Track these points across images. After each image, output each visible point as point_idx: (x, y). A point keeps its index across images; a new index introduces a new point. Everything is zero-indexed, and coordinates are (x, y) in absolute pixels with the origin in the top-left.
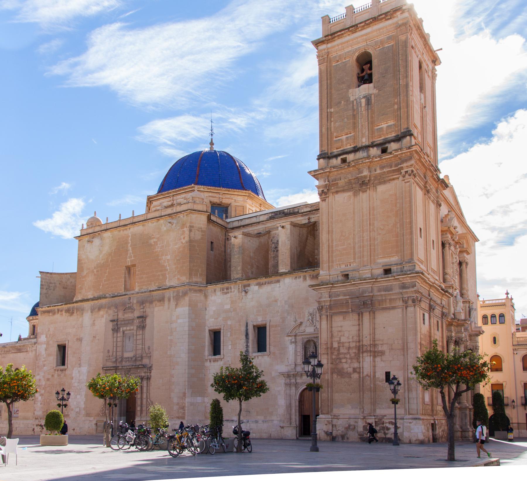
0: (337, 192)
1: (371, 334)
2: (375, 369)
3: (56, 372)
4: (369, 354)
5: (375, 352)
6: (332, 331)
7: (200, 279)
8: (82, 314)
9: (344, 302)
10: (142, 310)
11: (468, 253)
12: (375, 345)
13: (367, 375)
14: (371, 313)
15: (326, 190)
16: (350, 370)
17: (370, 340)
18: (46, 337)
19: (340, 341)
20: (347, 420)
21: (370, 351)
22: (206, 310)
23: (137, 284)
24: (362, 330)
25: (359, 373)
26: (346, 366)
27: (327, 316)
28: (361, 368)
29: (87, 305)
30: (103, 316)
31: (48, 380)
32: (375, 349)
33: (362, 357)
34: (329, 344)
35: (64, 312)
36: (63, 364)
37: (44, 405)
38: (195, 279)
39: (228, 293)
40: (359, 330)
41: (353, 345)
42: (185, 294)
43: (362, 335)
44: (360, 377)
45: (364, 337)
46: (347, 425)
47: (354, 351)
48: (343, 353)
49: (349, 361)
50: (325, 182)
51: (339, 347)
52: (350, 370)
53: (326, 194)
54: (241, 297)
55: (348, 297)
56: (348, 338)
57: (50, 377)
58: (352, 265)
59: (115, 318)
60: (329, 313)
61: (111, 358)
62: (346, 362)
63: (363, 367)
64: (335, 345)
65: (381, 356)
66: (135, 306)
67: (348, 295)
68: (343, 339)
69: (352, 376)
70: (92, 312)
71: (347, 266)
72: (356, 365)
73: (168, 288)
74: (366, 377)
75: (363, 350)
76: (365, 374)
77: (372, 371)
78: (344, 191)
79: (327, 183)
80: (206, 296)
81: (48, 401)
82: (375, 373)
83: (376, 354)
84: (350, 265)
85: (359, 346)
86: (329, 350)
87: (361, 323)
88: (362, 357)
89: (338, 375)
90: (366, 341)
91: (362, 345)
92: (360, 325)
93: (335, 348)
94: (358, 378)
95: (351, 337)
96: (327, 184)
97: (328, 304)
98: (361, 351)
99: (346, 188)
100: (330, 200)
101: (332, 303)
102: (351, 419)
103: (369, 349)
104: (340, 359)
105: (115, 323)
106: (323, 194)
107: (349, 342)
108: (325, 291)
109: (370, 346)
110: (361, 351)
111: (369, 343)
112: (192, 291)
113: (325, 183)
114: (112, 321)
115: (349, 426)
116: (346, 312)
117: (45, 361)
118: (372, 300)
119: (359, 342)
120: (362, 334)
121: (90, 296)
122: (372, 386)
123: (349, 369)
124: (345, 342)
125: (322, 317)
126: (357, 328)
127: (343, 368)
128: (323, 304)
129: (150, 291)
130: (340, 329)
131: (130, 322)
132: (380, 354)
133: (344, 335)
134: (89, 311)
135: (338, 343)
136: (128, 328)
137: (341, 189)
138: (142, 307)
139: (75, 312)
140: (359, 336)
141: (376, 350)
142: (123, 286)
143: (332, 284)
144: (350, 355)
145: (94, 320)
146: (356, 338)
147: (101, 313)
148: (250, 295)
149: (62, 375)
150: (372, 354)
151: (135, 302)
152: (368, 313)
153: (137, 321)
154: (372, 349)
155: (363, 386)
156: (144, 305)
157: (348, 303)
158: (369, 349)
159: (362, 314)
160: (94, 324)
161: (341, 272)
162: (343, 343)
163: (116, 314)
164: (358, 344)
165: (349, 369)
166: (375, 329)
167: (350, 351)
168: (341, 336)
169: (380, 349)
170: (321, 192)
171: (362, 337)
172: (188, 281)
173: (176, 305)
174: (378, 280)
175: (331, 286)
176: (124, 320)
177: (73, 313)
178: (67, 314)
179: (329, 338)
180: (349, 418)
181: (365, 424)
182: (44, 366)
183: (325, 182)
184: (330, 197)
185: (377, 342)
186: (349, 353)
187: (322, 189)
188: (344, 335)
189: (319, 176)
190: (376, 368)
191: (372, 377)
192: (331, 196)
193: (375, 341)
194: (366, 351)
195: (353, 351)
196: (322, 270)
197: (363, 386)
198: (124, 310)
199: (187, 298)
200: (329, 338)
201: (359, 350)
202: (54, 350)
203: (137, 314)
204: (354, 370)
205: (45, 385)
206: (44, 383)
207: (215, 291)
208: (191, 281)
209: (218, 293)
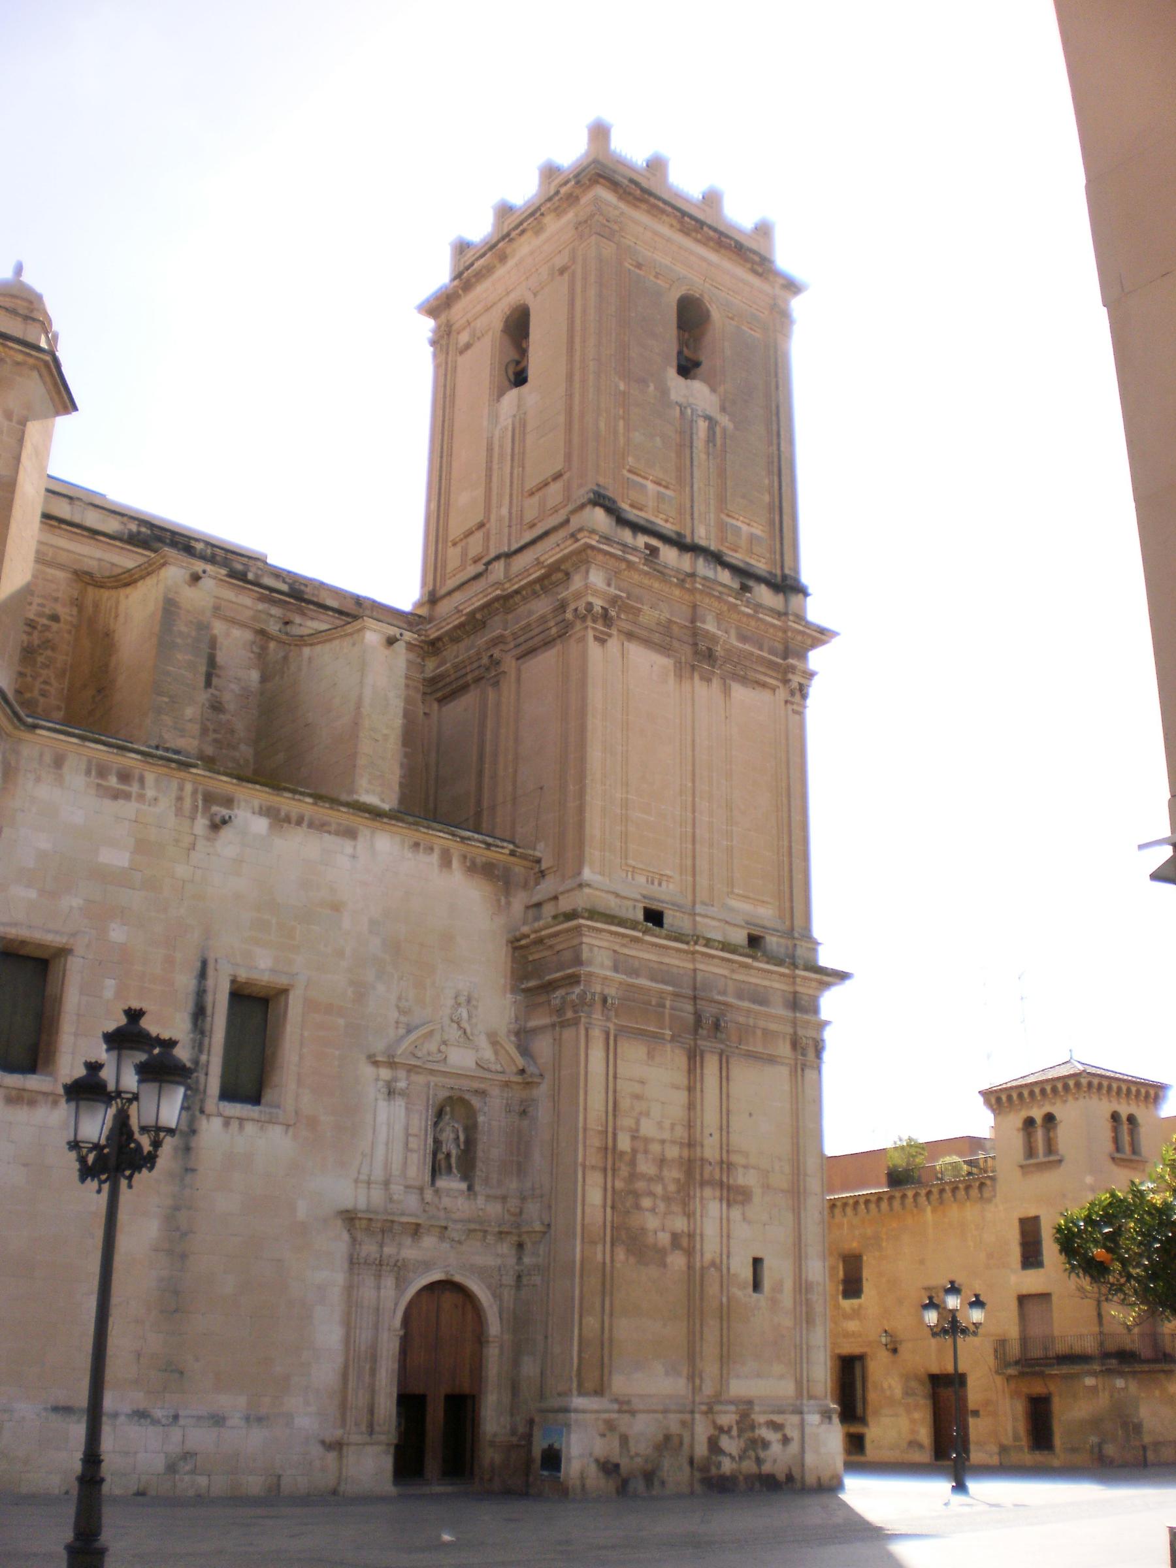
0: (630, 636)
4: (718, 1194)
13: (713, 1264)
16: (664, 1238)
19: (637, 1130)
20: (660, 1416)
21: (721, 1184)
26: (652, 1223)
27: (607, 1034)
33: (702, 1198)
39: (127, 796)
40: (691, 1106)
41: (673, 1152)
45: (707, 1132)
46: (660, 1437)
48: (643, 1176)
49: (661, 1206)
51: (634, 1151)
52: (664, 1238)
54: (187, 840)
55: (671, 989)
56: (660, 1125)
58: (664, 884)
60: (612, 1026)
62: (653, 1210)
63: (702, 1235)
64: (624, 1143)
65: (743, 1203)
68: (648, 1128)
69: (669, 1259)
71: (653, 883)
72: (679, 1224)
75: (702, 1174)
76: (708, 1256)
78: (647, 642)
83: (734, 1195)
84: (660, 884)
85: (690, 1161)
88: (702, 1198)
89: (629, 1251)
90: (710, 1150)
91: (702, 1159)
92: (692, 1088)
93: (622, 1153)
94: (684, 1268)
95: (667, 1124)
102: (672, 1416)
104: (636, 1195)
107: (663, 1142)
108: (605, 944)
115: (667, 1438)
116: (655, 1036)
119: (691, 1145)
120: (702, 1123)
122: (724, 1300)
123: (661, 1235)
124: (653, 1140)
125: (590, 1032)
126: (682, 1097)
127: (643, 1230)
130: (637, 1089)
132: (740, 1198)
133: (647, 1114)
135: (634, 1138)
137: (644, 633)
140: (690, 1126)
144: (665, 1188)
146: (681, 1133)
148: (228, 843)
155: (702, 1299)
157: (664, 1006)
158: (717, 1177)
161: (644, 897)
162: (647, 1141)
164: (685, 1153)
165: (661, 1235)
168: (641, 1113)
169: (742, 1178)
171: (702, 1132)
180: (665, 1411)
181: (712, 1431)
185: (735, 1158)
186: (660, 1178)
188: (648, 1114)
189: (600, 557)
195: (673, 1174)
201: (689, 1173)
207: (59, 762)
209: (76, 779)
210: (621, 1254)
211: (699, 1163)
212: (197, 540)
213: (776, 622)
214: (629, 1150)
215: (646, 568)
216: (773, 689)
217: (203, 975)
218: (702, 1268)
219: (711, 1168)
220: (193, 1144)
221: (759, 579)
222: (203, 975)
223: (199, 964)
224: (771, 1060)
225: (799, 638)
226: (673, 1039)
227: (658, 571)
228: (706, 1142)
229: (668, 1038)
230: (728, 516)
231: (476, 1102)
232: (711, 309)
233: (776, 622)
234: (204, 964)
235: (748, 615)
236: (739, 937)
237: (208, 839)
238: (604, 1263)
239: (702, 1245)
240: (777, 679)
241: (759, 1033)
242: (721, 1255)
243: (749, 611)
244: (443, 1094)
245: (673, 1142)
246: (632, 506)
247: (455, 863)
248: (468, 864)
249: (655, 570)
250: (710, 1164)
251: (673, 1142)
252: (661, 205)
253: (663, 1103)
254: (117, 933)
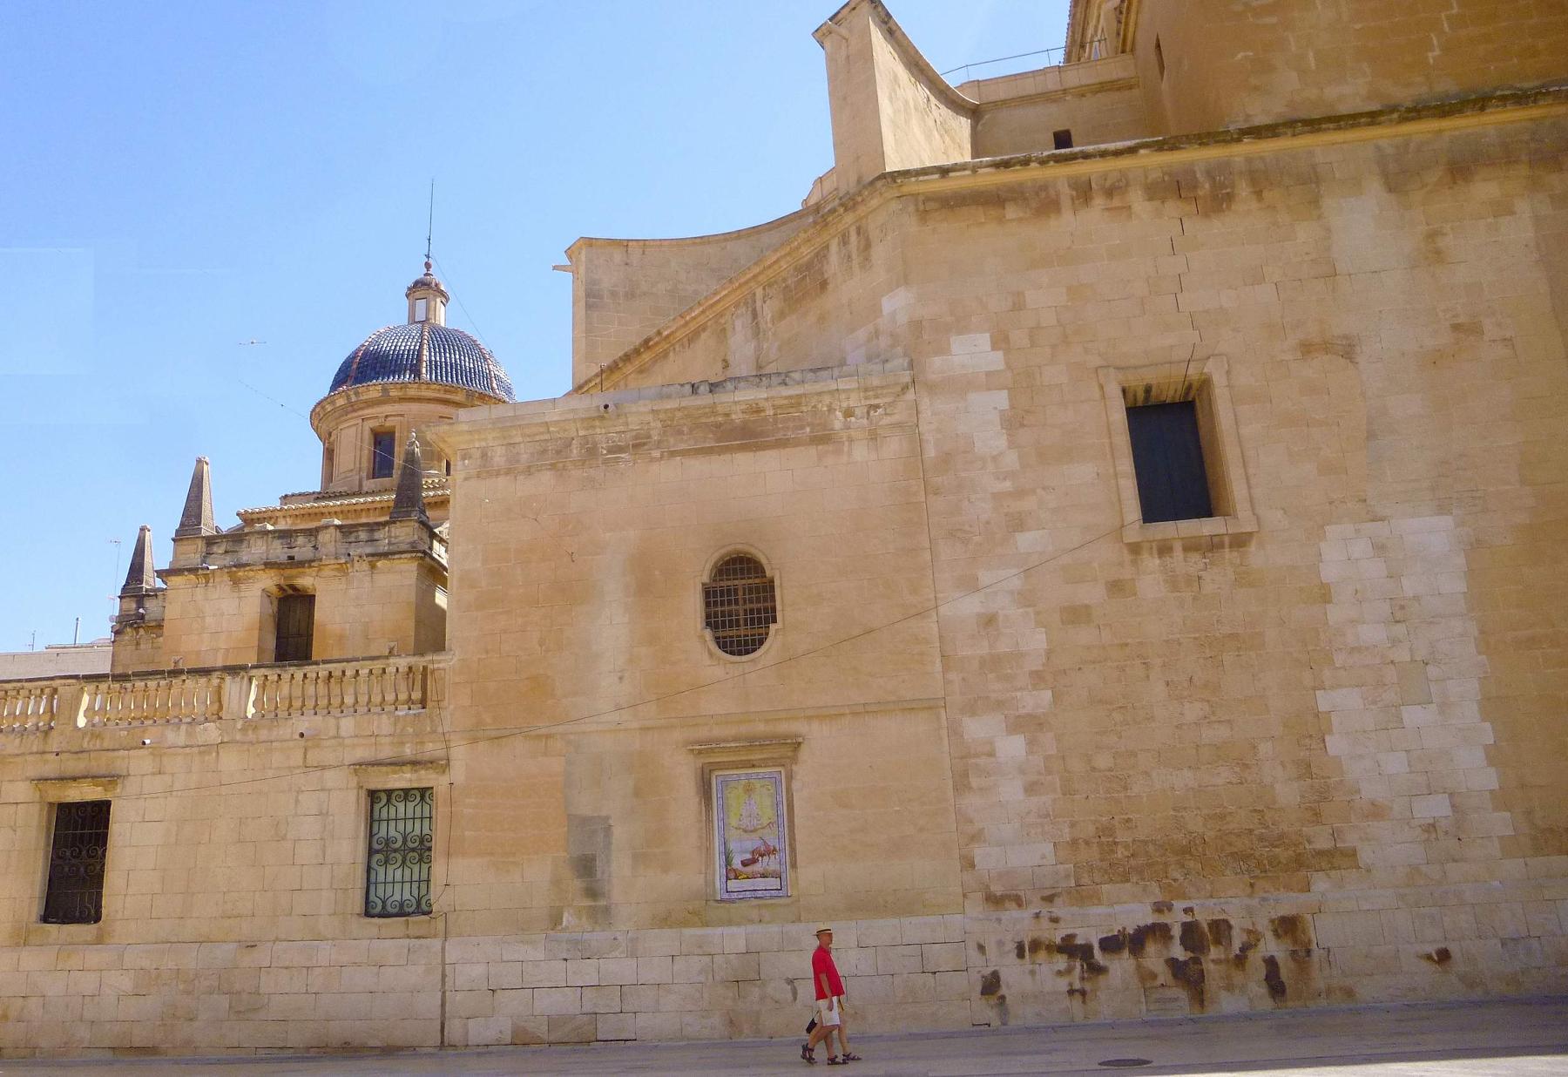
3: (1152, 562)
8: (1315, 202)
30: (1503, 209)
31: (1076, 615)
35: (1136, 198)
37: (1068, 791)
57: (1091, 594)
81: (1103, 761)
117: (1020, 493)
134: (1375, 186)
139: (1243, 190)
145: (1432, 236)
147: (1485, 189)
149: (1218, 576)
160: (1438, 252)
178: (1173, 208)
182: (1018, 523)
205: (1049, 653)
206: (1036, 642)
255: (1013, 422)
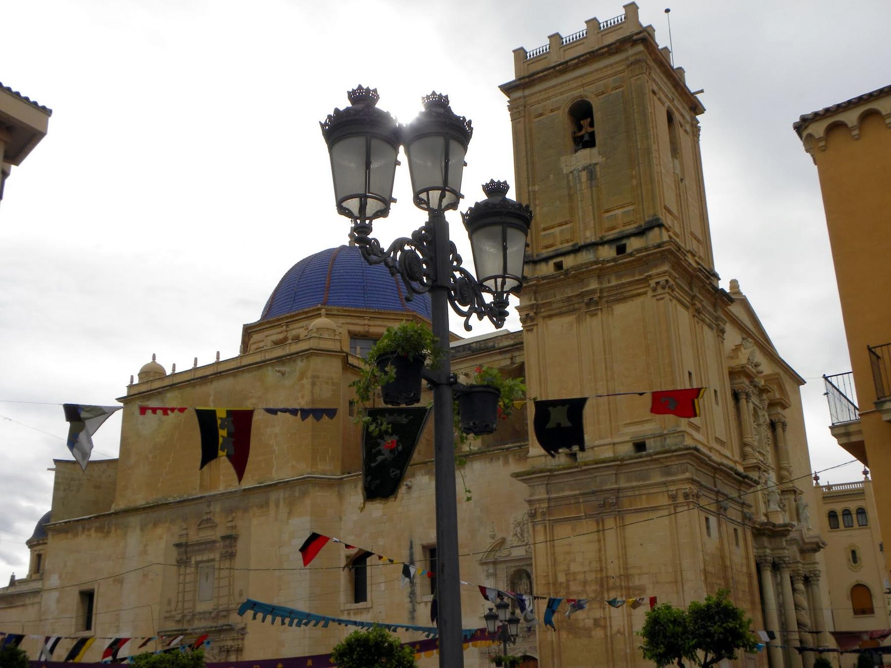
0: (550, 317)
1: (621, 555)
2: (631, 619)
5: (628, 588)
6: (554, 554)
7: (329, 468)
8: (125, 534)
9: (573, 501)
10: (230, 524)
11: (784, 407)
12: (628, 577)
13: (619, 632)
14: (618, 519)
15: (532, 314)
16: (589, 623)
17: (619, 568)
18: (60, 578)
19: (569, 570)
21: (621, 588)
22: (341, 520)
23: (221, 477)
24: (605, 551)
25: (605, 627)
27: (545, 527)
28: (608, 619)
29: (134, 521)
30: (161, 538)
32: (628, 582)
34: (550, 577)
36: (88, 626)
38: (320, 467)
40: (600, 550)
41: (591, 577)
42: (304, 494)
43: (606, 560)
44: (606, 636)
47: (594, 587)
50: (530, 300)
51: (568, 581)
52: (589, 623)
53: (532, 319)
59: (183, 540)
61: (173, 613)
63: (610, 617)
64: (562, 578)
66: (217, 519)
67: (578, 489)
68: (574, 568)
69: (593, 633)
70: (142, 530)
73: (275, 484)
74: (616, 634)
75: (608, 585)
76: (615, 629)
77: (626, 622)
78: (561, 314)
79: (533, 302)
80: (341, 496)
82: (632, 627)
85: (602, 579)
86: (551, 587)
87: (602, 538)
90: (613, 569)
91: (607, 577)
93: (561, 583)
96: (533, 305)
97: (545, 505)
98: (606, 586)
99: (564, 309)
100: (540, 330)
101: (552, 504)
103: (618, 584)
105: (183, 549)
106: (529, 321)
107: (585, 572)
109: (620, 579)
110: (606, 586)
111: (618, 574)
112: (317, 488)
113: (531, 303)
114: (178, 546)
118: (617, 498)
119: (601, 570)
121: (140, 502)
123: (587, 621)
124: (578, 573)
128: (537, 506)
129: (245, 490)
131: (209, 545)
132: (638, 592)
133: (574, 560)
135: (566, 574)
136: (205, 558)
137: (557, 311)
138: (230, 518)
140: (601, 561)
141: (631, 585)
142: (198, 481)
143: (550, 470)
146: (595, 565)
147: (159, 531)
150: (624, 593)
151: (218, 509)
152: (613, 519)
153: (220, 545)
154: (623, 584)
155: (612, 651)
156: (234, 515)
158: (618, 584)
159: (603, 521)
162: (574, 573)
163: (185, 532)
164: (599, 576)
165: (587, 621)
166: (625, 548)
167: (588, 588)
169: (636, 582)
170: (524, 317)
171: (606, 563)
172: (309, 470)
173: (290, 513)
174: (626, 462)
175: (548, 473)
176: (199, 544)
177: (109, 532)
178: (100, 535)
179: (550, 567)
183: (530, 300)
184: (539, 325)
185: (631, 571)
187: (525, 313)
188: (574, 560)
190: (633, 617)
191: (627, 634)
192: (540, 321)
193: (627, 568)
194: (613, 588)
196: (532, 446)
197: (612, 651)
198: (199, 525)
199: (308, 501)
200: (550, 567)
201: (602, 586)
202: (73, 600)
203: (220, 532)
204: (596, 622)
208: (314, 470)
210: (564, 635)
211: (605, 579)
212: (472, 343)
213: (631, 259)
214: (565, 581)
215: (545, 281)
216: (645, 293)
217: (411, 547)
218: (611, 635)
219: (613, 580)
220: (415, 615)
221: (628, 236)
222: (411, 547)
223: (409, 544)
224: (655, 509)
225: (651, 257)
226: (586, 517)
227: (552, 278)
228: (608, 567)
229: (584, 517)
230: (607, 212)
231: (528, 569)
232: (588, 100)
233: (631, 259)
234: (411, 543)
235: (613, 266)
236: (627, 449)
237: (407, 493)
238: (552, 642)
239: (610, 622)
240: (646, 287)
241: (644, 497)
242: (624, 626)
243: (613, 263)
244: (512, 570)
245: (591, 571)
246: (547, 247)
247: (511, 460)
248: (517, 458)
249: (549, 279)
250: (613, 578)
251: (591, 571)
252: (541, 75)
253: (583, 552)
254: (381, 542)
255: (58, 601)
